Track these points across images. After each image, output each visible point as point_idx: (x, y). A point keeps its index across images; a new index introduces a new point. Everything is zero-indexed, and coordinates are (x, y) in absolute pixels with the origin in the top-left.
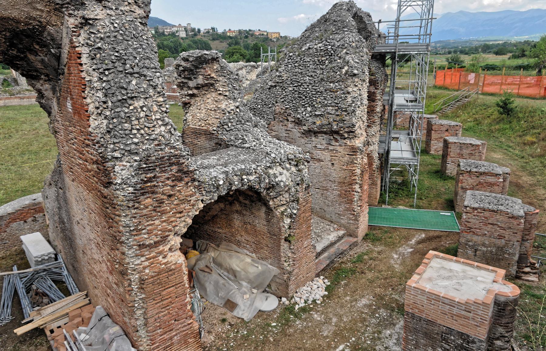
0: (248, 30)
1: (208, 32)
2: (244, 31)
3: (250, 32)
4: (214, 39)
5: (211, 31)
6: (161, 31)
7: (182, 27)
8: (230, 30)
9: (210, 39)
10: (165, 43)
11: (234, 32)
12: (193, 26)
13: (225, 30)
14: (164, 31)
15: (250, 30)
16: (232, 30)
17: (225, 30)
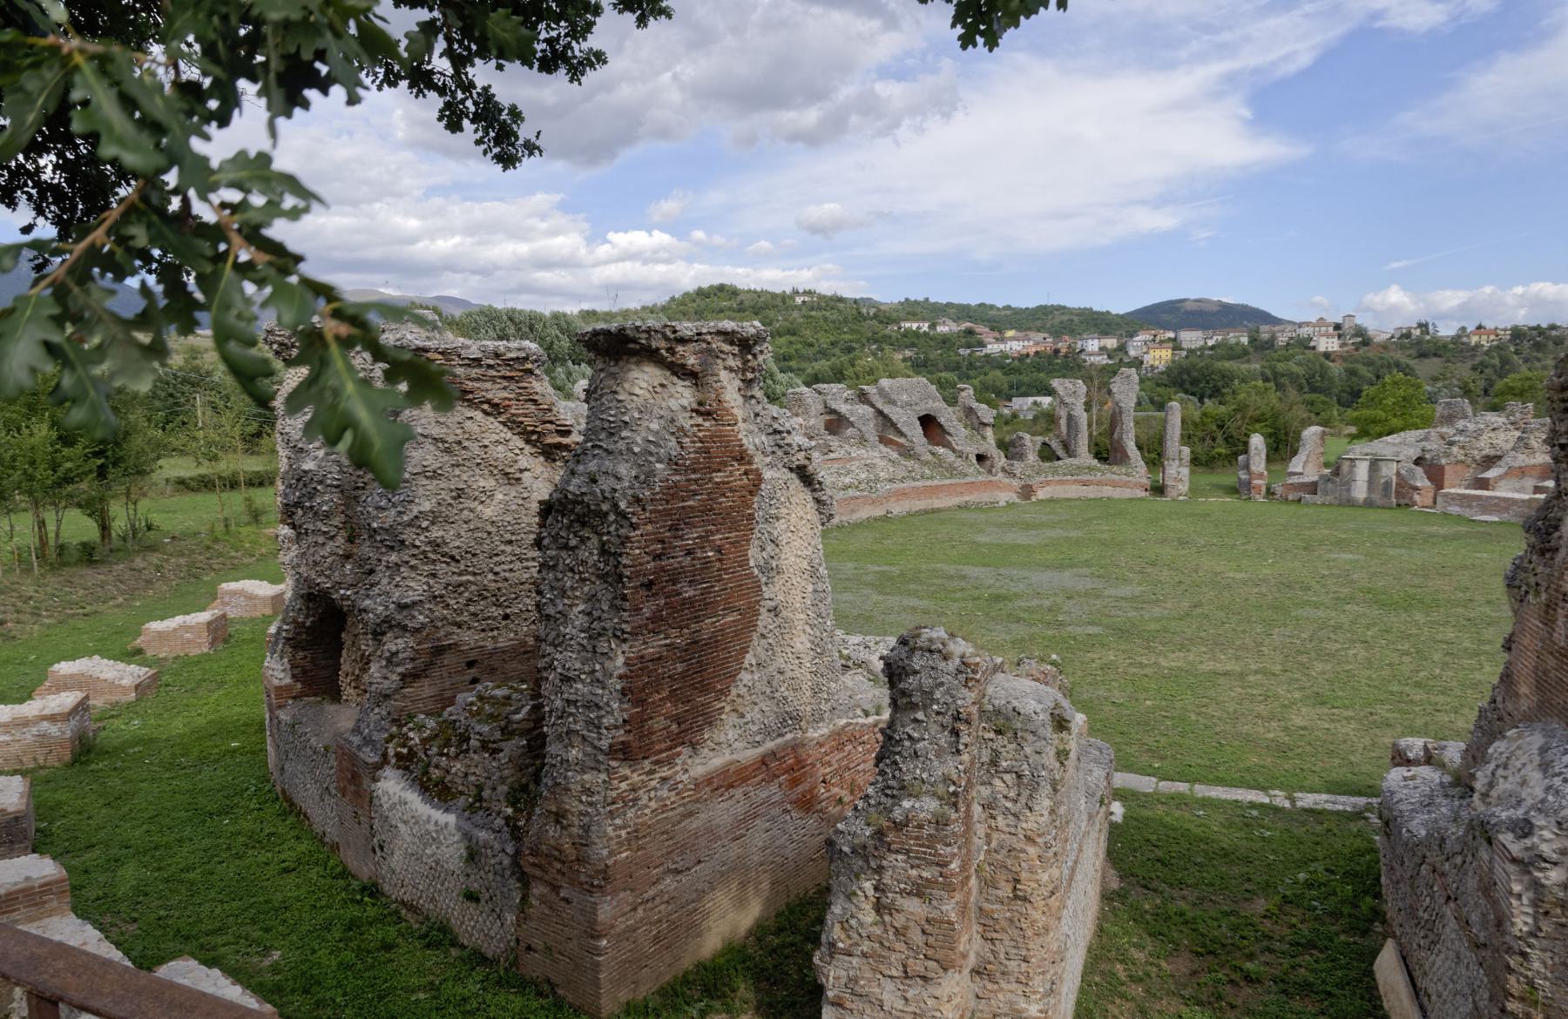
0: (1544, 325)
1: (1408, 335)
2: (1531, 329)
3: (1554, 333)
4: (1422, 355)
5: (1418, 332)
6: (1265, 336)
7: (1328, 325)
8: (1480, 327)
9: (1409, 356)
10: (1281, 367)
11: (1495, 331)
12: (1358, 321)
13: (1463, 329)
14: (1273, 338)
15: (1553, 327)
16: (1489, 325)
17: (1463, 329)
